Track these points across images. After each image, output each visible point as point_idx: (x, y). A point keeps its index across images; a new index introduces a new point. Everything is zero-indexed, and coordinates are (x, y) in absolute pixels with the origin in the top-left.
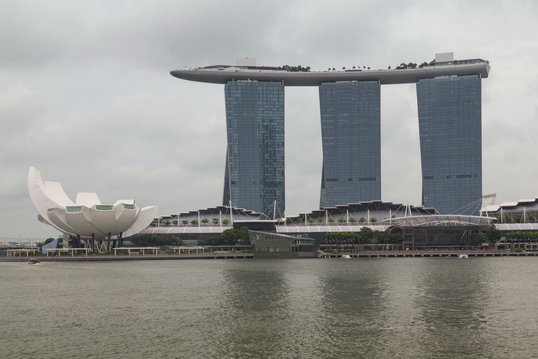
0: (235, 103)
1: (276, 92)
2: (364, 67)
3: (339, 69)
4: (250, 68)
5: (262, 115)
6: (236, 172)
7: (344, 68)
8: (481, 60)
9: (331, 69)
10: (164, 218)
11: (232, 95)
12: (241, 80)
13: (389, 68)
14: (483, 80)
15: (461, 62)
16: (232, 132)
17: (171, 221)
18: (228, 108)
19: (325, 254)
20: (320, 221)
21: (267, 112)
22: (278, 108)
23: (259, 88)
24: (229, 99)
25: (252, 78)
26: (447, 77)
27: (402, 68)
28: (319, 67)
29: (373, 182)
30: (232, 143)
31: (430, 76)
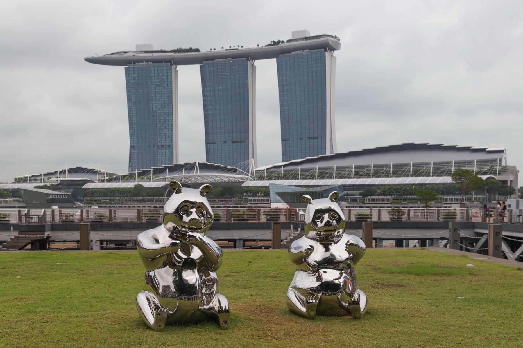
0: (133, 81)
1: (165, 71)
3: (219, 49)
5: (155, 90)
6: (135, 137)
7: (223, 48)
10: (33, 176)
11: (130, 75)
12: (138, 62)
13: (258, 45)
16: (131, 105)
17: (39, 178)
18: (128, 86)
19: (82, 205)
20: (143, 179)
21: (158, 88)
22: (168, 85)
23: (151, 69)
24: (128, 78)
25: (147, 61)
26: (301, 51)
27: (272, 45)
29: (243, 144)
30: (131, 115)
31: (288, 51)
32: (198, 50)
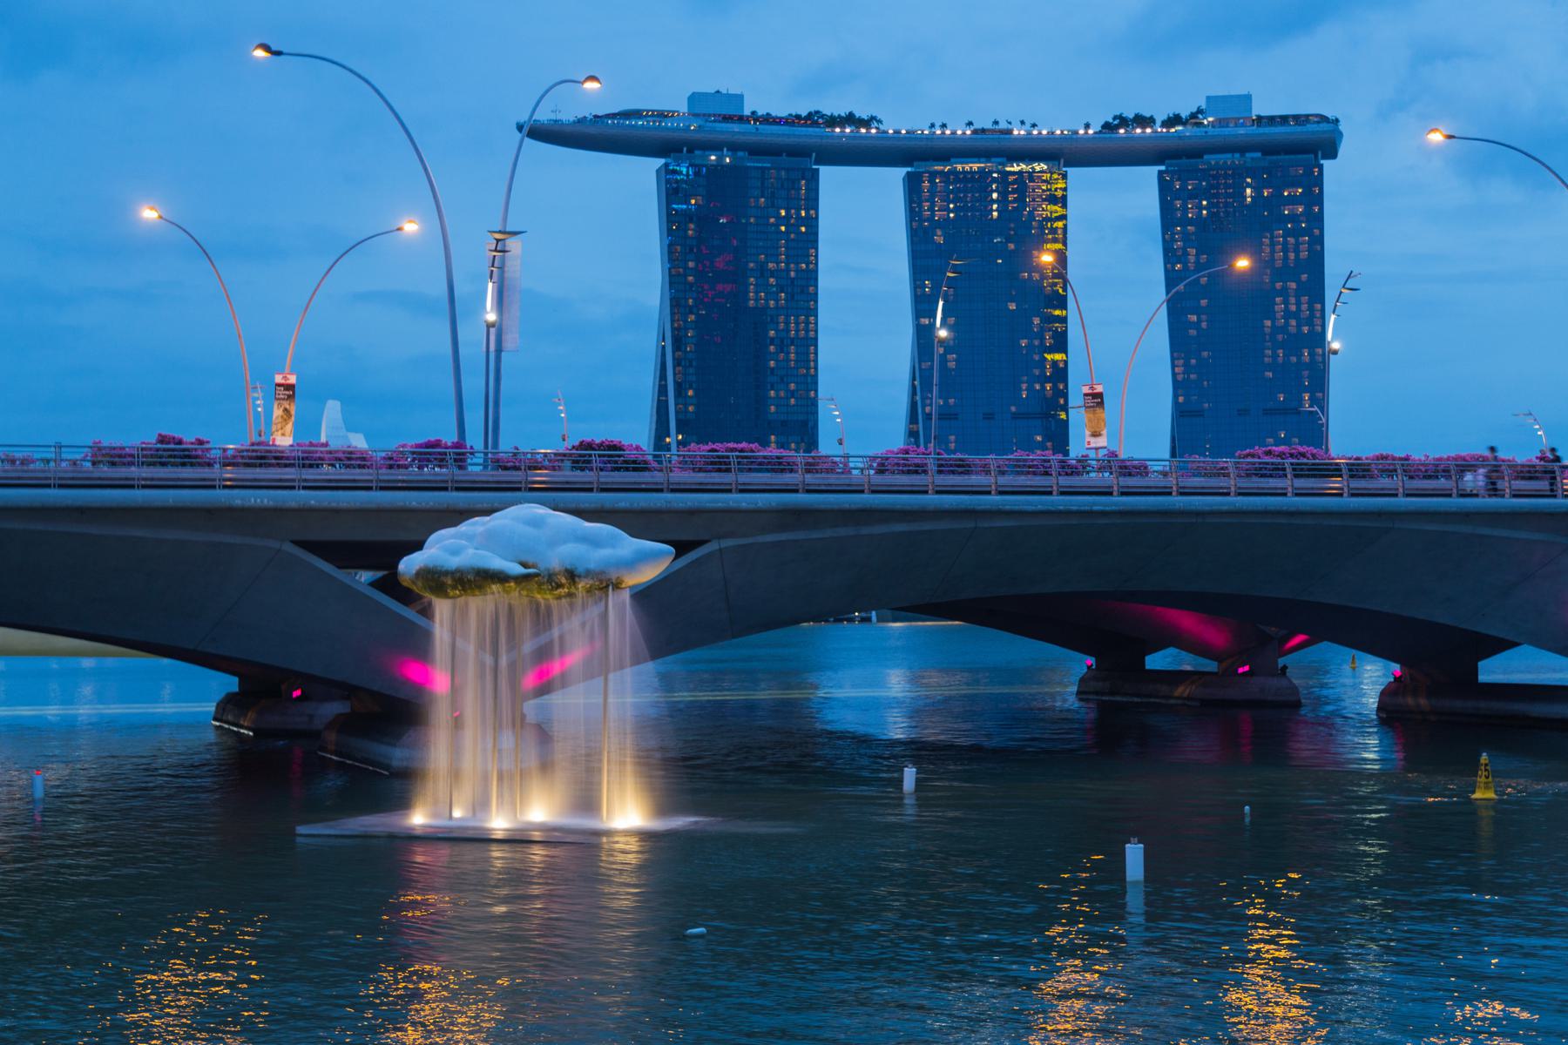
2: (1022, 123)
4: (727, 118)
7: (970, 124)
8: (1323, 119)
9: (938, 124)
14: (1327, 164)
15: (1272, 120)
28: (900, 119)
32: (866, 123)
